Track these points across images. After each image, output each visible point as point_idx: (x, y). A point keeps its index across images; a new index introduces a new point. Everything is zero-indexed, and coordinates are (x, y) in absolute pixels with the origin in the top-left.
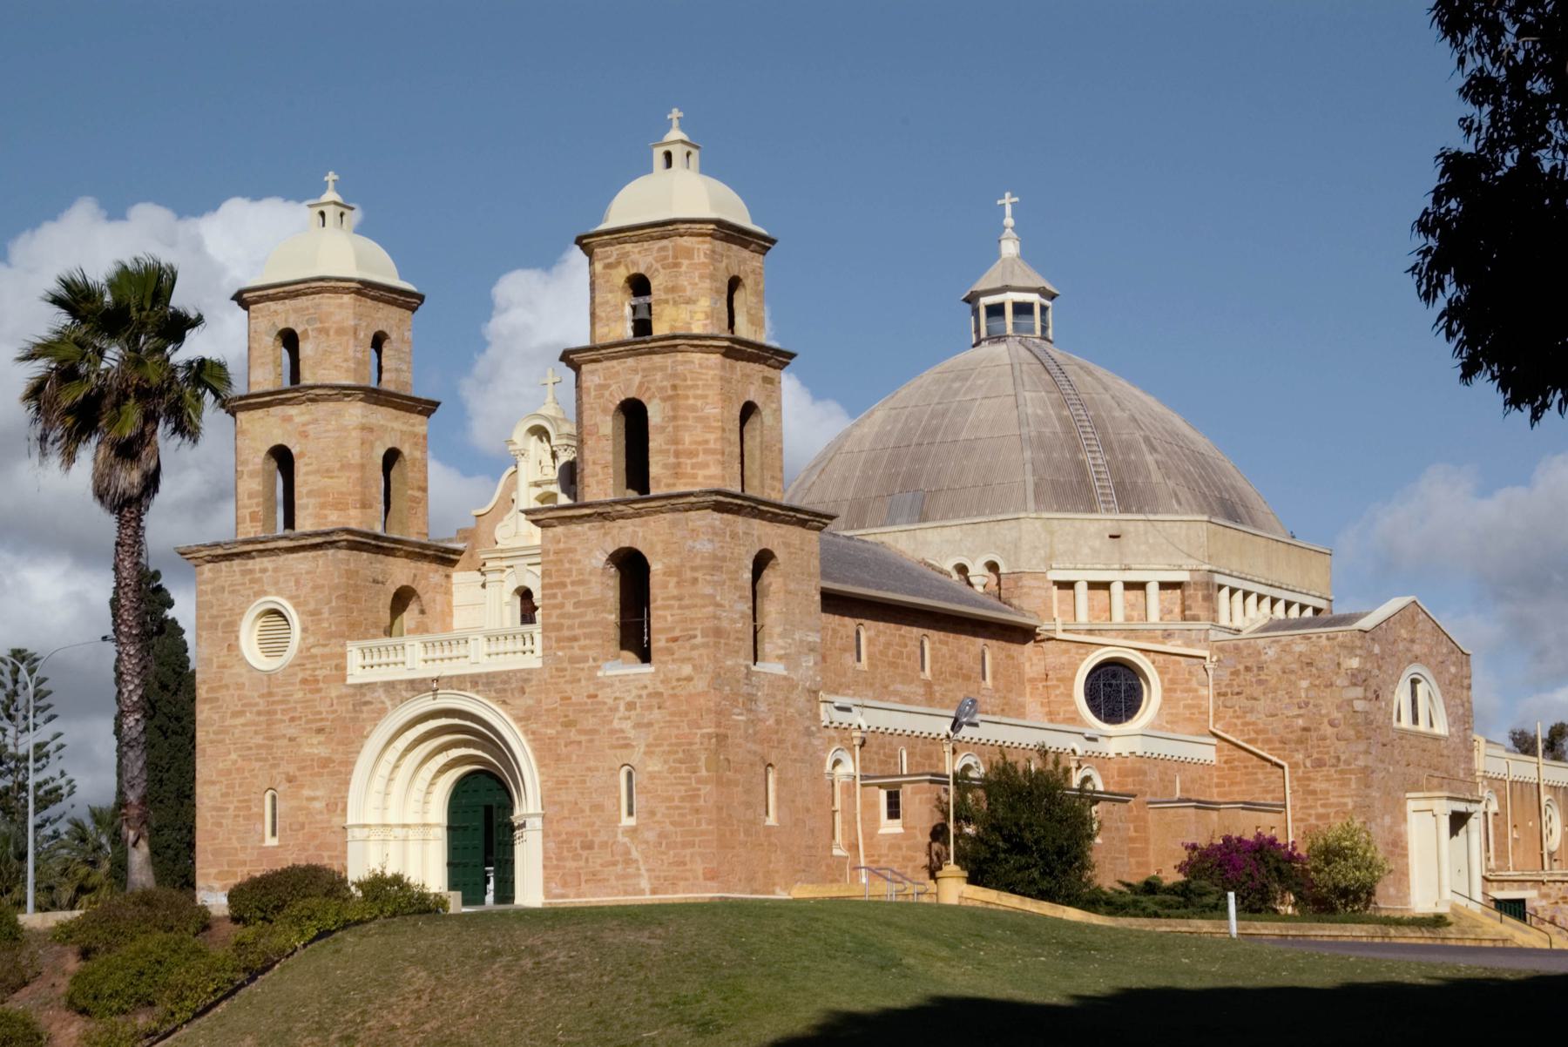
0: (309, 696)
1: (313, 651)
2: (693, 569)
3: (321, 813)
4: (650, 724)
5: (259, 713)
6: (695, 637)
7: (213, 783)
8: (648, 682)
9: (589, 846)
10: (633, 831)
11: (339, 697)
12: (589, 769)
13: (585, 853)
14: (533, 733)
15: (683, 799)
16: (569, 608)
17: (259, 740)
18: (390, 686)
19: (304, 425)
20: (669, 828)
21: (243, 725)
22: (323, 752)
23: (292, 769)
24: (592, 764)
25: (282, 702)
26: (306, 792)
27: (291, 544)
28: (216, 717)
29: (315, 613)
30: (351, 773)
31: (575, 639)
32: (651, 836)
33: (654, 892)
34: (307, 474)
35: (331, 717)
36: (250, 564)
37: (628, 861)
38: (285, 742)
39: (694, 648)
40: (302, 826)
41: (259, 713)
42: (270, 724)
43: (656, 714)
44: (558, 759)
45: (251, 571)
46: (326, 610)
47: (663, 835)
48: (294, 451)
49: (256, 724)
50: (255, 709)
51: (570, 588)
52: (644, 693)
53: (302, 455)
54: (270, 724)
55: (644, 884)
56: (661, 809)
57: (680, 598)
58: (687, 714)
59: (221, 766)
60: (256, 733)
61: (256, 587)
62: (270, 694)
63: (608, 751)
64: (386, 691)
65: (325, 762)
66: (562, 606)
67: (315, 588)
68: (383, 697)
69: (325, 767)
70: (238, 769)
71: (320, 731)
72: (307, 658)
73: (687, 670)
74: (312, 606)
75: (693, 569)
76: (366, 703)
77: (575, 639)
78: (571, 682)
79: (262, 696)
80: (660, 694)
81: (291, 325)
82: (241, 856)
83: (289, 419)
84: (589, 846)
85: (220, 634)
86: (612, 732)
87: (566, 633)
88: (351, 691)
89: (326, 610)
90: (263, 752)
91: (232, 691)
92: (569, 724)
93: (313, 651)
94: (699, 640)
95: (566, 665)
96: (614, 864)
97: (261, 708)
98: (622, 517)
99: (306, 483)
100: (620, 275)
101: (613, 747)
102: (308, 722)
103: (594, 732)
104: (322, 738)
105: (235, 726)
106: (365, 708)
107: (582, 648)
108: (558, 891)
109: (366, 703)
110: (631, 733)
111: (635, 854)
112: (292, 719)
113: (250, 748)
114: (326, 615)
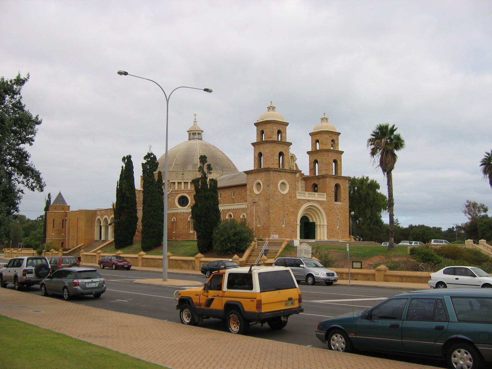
0: (290, 200)
1: (291, 191)
2: (346, 189)
3: (292, 221)
4: (341, 212)
5: (282, 201)
6: (346, 199)
7: (273, 214)
8: (340, 205)
9: (333, 231)
10: (339, 229)
11: (295, 201)
12: (333, 218)
13: (332, 232)
14: (326, 211)
15: (345, 224)
16: (330, 191)
17: (281, 206)
18: (304, 200)
19: (286, 149)
20: (343, 229)
21: (279, 203)
22: (292, 210)
23: (288, 213)
24: (333, 217)
25: (285, 200)
26: (290, 217)
27: (290, 171)
28: (274, 201)
29: (291, 185)
30: (298, 214)
31: (331, 197)
32: (341, 230)
33: (341, 239)
34: (287, 158)
35: (294, 204)
36: (280, 173)
37: (338, 233)
38: (286, 208)
39: (346, 201)
40: (289, 223)
41: (282, 201)
42: (283, 204)
43: (342, 211)
44: (329, 216)
45: (280, 174)
46: (293, 184)
47: (342, 230)
48: (284, 154)
49: (281, 203)
50: (281, 201)
51: (330, 188)
52: (340, 207)
53: (286, 154)
54: (283, 204)
55: (340, 237)
56: (342, 225)
57: (345, 193)
58: (345, 211)
59: (274, 210)
60: (281, 205)
61: (281, 178)
62: (284, 198)
63: (336, 216)
64: (303, 201)
65: (293, 212)
66: (329, 191)
67: (291, 180)
68: (303, 202)
69: (293, 213)
70: (278, 211)
71: (292, 206)
72: (290, 193)
73: (345, 204)
74: (291, 183)
75: (346, 189)
76: (300, 202)
77: (331, 197)
78: (331, 204)
79: (282, 198)
80: (342, 208)
81: (281, 129)
82: (278, 228)
83: (283, 147)
84: (333, 231)
85: (274, 185)
86: (336, 213)
87: (330, 195)
88: (298, 200)
89: (293, 184)
90: (282, 209)
91: (276, 196)
92: (330, 210)
93: (291, 191)
94: (347, 200)
95: (330, 201)
96: (336, 234)
97: (282, 200)
98: (338, 179)
99: (286, 160)
100: (331, 139)
101: (336, 215)
102: (290, 204)
103: (333, 212)
104: (292, 207)
105: (277, 203)
106: (300, 203)
107: (332, 198)
108: (329, 238)
109: (300, 202)
110: (339, 213)
111: (339, 233)
112: (287, 203)
113: (280, 208)
114: (293, 185)
